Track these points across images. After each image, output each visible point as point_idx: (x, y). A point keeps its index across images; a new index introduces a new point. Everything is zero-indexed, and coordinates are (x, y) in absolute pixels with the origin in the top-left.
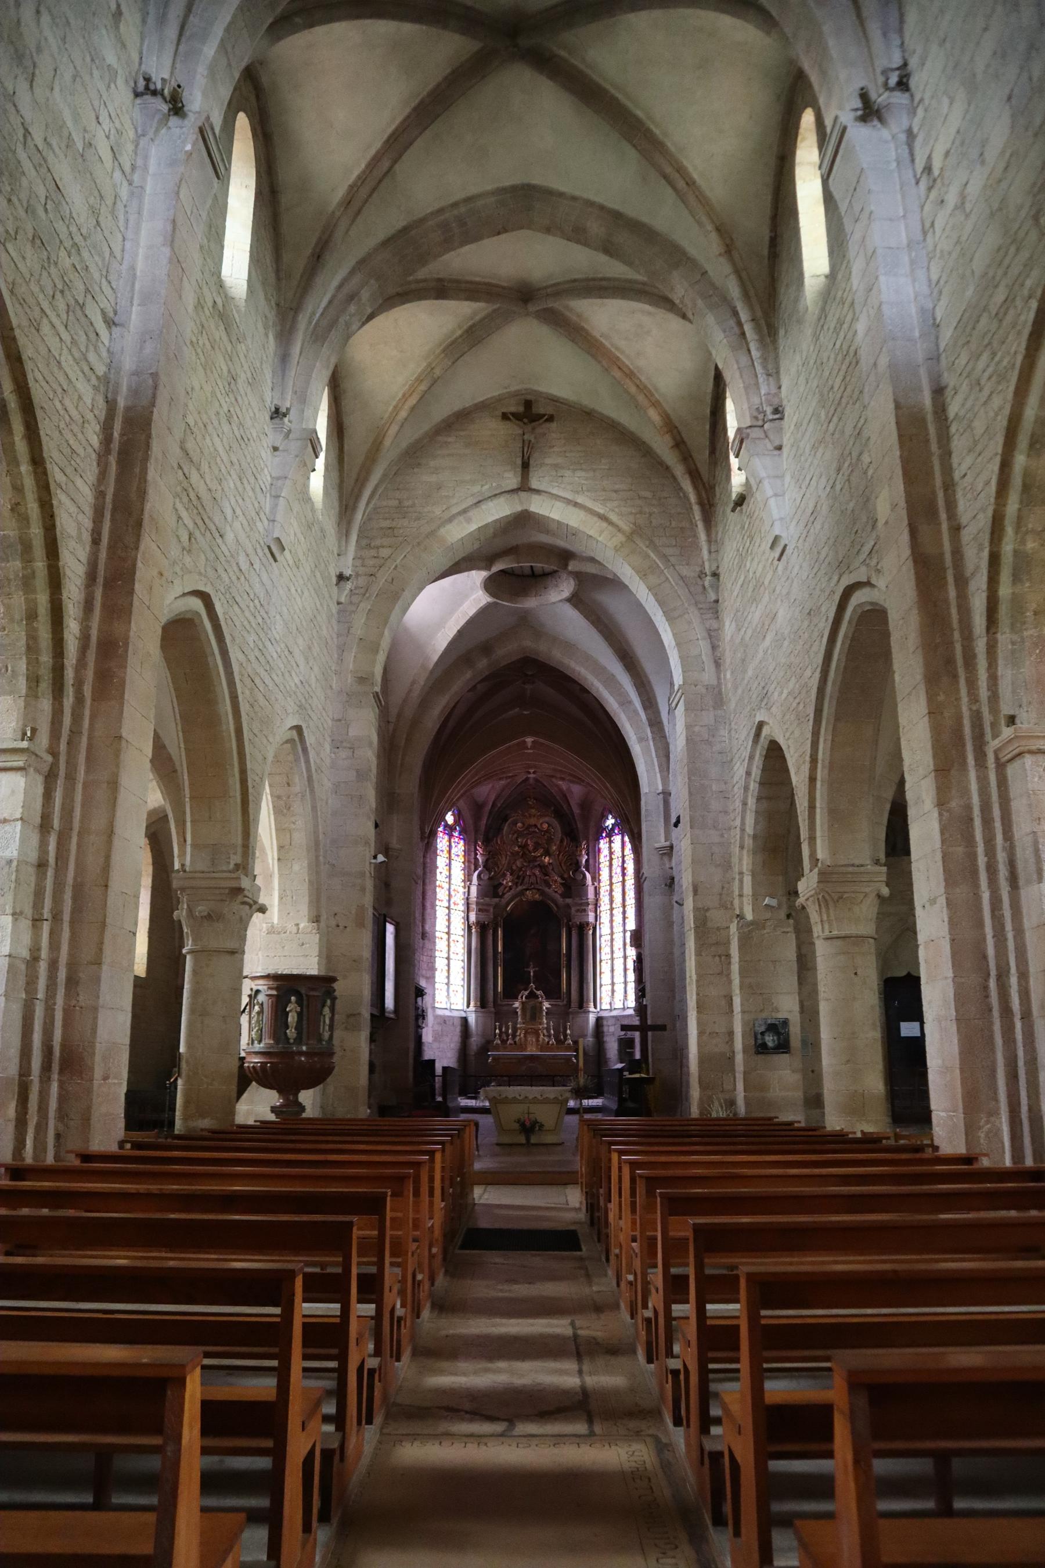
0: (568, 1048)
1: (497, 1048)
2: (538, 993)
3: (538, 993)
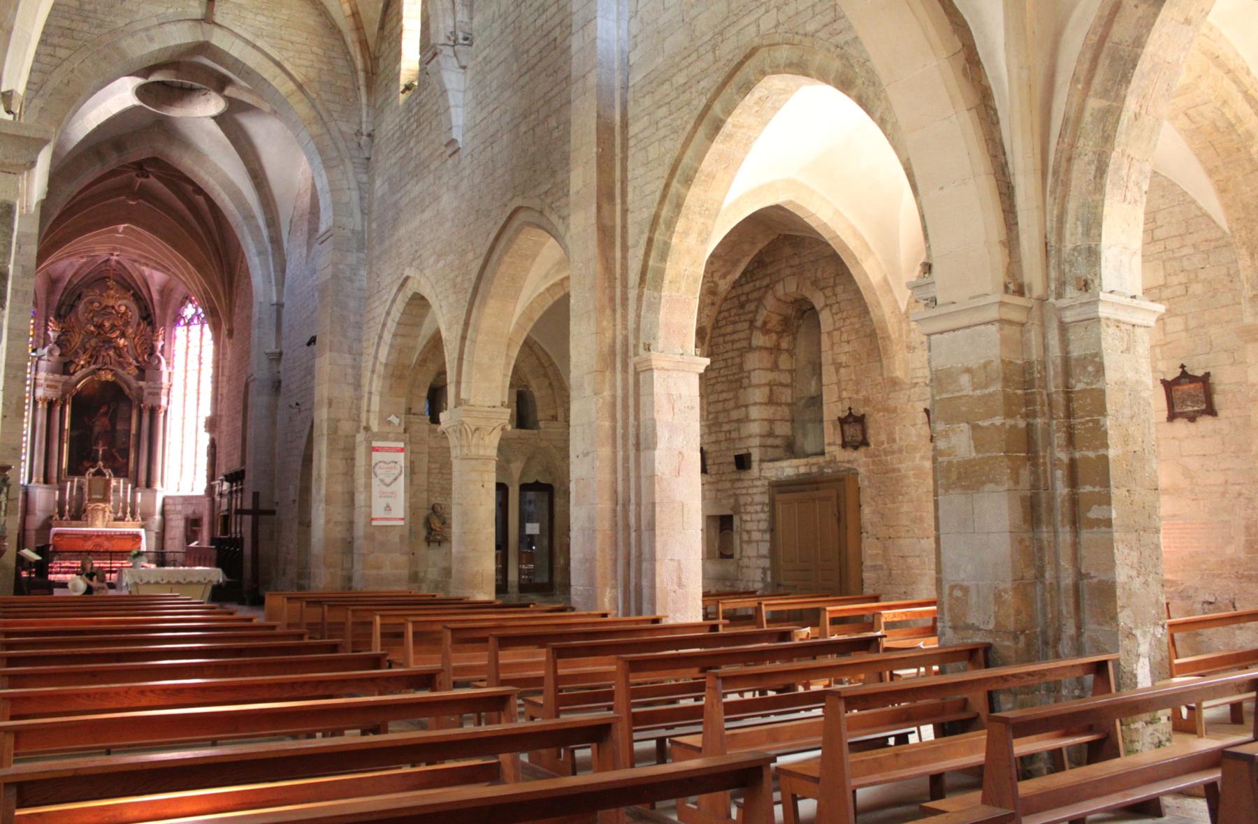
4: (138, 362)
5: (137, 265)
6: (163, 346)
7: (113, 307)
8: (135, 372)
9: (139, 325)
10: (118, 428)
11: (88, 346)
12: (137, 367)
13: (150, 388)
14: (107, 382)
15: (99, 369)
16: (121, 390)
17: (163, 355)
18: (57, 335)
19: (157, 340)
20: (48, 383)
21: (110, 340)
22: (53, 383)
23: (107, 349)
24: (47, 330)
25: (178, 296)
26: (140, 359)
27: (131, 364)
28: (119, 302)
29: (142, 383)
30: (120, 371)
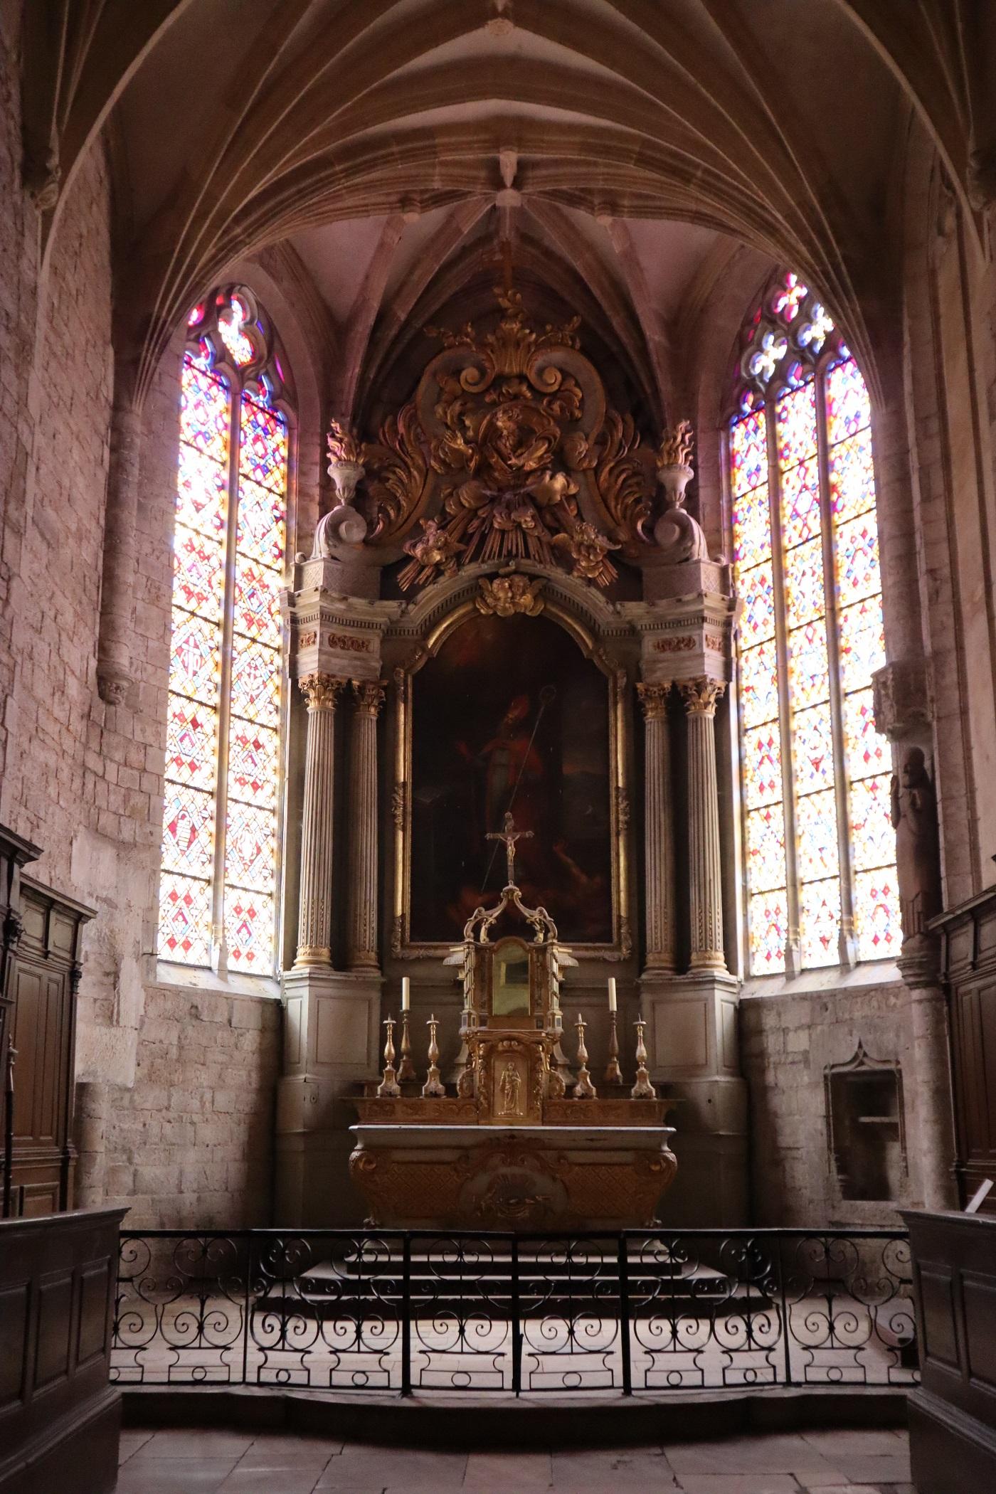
0: (642, 1110)
1: (385, 1109)
2: (535, 915)
3: (535, 915)
4: (612, 539)
5: (580, 215)
6: (692, 486)
7: (522, 378)
8: (607, 576)
9: (610, 423)
10: (569, 769)
11: (451, 509)
12: (610, 556)
13: (661, 623)
14: (521, 618)
15: (492, 577)
16: (567, 643)
17: (694, 511)
18: (355, 475)
19: (672, 465)
20: (339, 631)
21: (522, 475)
22: (349, 632)
23: (509, 508)
24: (326, 463)
25: (725, 323)
26: (623, 536)
27: (591, 548)
28: (539, 361)
29: (634, 610)
30: (558, 573)
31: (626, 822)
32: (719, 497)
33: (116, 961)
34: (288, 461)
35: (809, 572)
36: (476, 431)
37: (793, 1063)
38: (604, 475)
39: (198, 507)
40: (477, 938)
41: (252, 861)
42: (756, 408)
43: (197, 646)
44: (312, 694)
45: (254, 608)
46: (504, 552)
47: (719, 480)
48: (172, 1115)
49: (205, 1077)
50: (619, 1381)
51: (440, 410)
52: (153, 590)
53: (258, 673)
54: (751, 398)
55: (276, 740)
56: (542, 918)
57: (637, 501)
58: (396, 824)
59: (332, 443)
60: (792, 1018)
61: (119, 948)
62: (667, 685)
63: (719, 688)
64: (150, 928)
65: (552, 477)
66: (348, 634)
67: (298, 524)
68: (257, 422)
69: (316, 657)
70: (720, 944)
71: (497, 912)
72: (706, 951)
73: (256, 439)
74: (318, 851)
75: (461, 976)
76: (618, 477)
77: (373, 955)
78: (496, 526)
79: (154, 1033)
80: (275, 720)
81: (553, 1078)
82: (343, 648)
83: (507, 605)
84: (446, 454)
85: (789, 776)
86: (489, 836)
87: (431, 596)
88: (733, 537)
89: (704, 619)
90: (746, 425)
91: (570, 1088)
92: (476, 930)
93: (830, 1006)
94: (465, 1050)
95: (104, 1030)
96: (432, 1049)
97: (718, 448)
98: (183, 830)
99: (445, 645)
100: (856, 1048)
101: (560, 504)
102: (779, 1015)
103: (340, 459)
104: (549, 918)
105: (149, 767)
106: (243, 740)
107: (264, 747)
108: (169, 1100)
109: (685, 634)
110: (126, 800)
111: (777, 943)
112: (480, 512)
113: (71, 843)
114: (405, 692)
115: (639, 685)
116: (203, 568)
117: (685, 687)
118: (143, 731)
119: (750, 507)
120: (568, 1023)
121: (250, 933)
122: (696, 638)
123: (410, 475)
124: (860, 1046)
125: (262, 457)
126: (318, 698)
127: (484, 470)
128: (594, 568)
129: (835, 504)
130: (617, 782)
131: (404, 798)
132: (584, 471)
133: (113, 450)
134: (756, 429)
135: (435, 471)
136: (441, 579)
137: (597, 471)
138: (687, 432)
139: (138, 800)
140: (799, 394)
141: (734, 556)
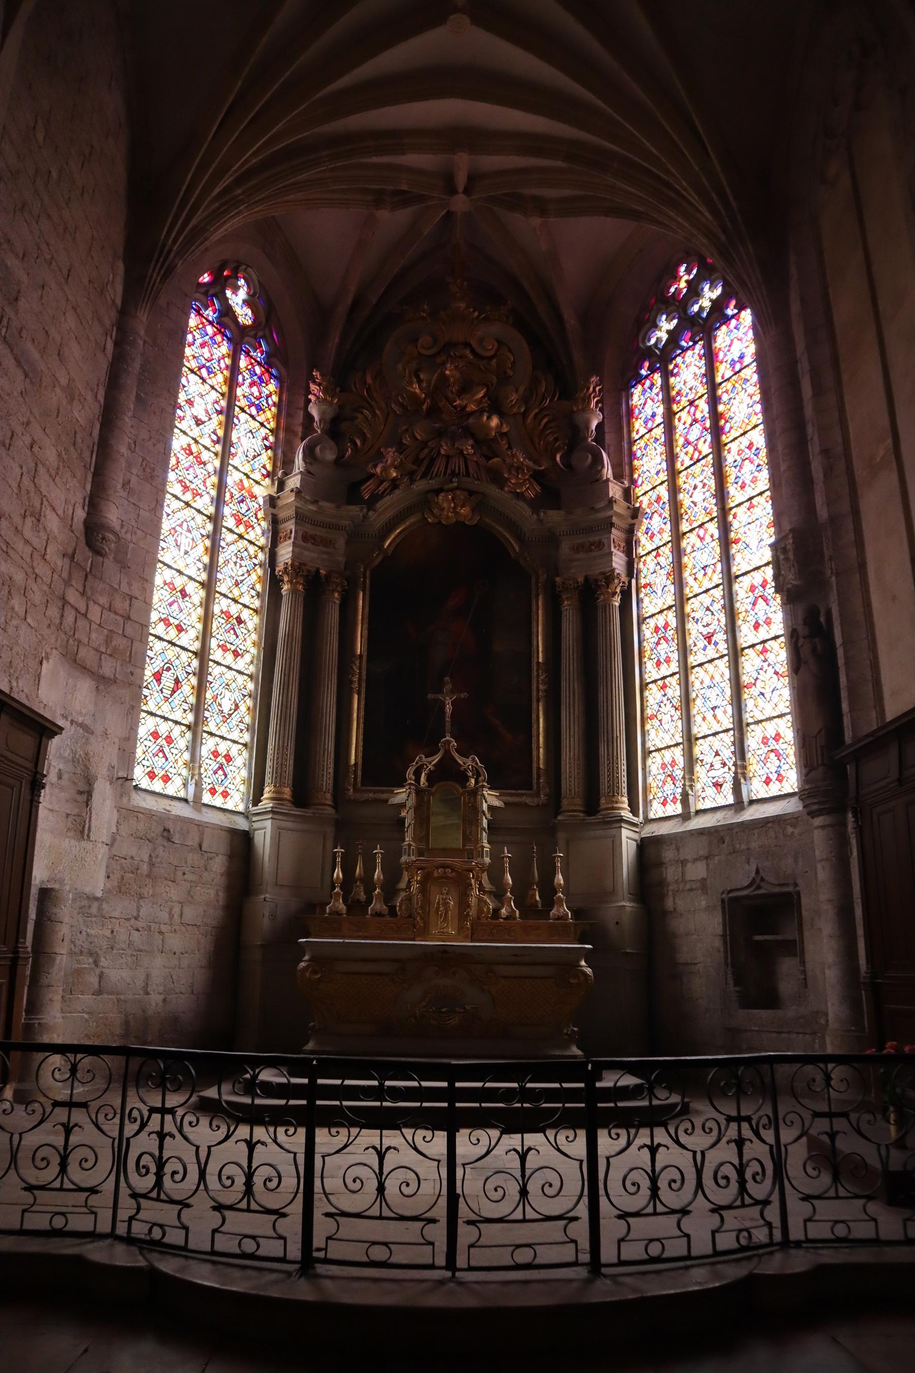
0: (560, 930)
1: (333, 925)
2: (468, 763)
3: (468, 763)
6: (600, 426)
7: (467, 345)
11: (407, 440)
15: (438, 492)
19: (586, 408)
22: (320, 532)
30: (493, 490)
31: (545, 691)
32: (621, 439)
33: (89, 781)
34: (278, 405)
35: (700, 485)
36: (429, 383)
37: (691, 890)
38: (529, 420)
39: (199, 422)
40: (418, 780)
41: (230, 715)
42: (652, 370)
43: (189, 531)
44: (286, 579)
45: (243, 511)
46: (449, 471)
47: (621, 428)
48: (140, 924)
49: (175, 893)
50: (585, 1258)
51: (400, 366)
52: (148, 470)
53: (243, 563)
54: (647, 364)
55: (256, 619)
56: (474, 764)
57: (556, 439)
58: (352, 688)
59: (313, 387)
60: (688, 852)
61: (93, 770)
62: (581, 580)
63: (623, 582)
64: (127, 757)
65: (489, 418)
66: (318, 533)
67: (283, 452)
68: (254, 371)
69: (291, 549)
70: (625, 791)
71: (436, 759)
72: (614, 796)
73: (252, 384)
74: (284, 707)
75: (403, 814)
76: (543, 418)
77: (329, 796)
78: (443, 453)
79: (127, 848)
80: (257, 603)
81: (480, 900)
82: (313, 544)
83: (450, 514)
84: (403, 398)
85: (684, 650)
86: (430, 696)
87: (388, 506)
88: (632, 469)
89: (612, 525)
90: (643, 385)
91: (496, 911)
92: (417, 774)
93: (727, 839)
94: (406, 876)
95: (73, 842)
96: (378, 874)
97: (620, 404)
98: (168, 680)
99: (398, 546)
100: (753, 874)
101: (495, 438)
102: (678, 849)
103: (318, 398)
104: (480, 764)
105: (133, 616)
106: (227, 615)
107: (245, 624)
108: (138, 911)
109: (596, 539)
110: (108, 640)
111: (673, 789)
112: (429, 444)
113: (41, 663)
114: (364, 582)
115: (558, 579)
116: (199, 470)
117: (596, 581)
118: (129, 584)
119: (647, 445)
120: (496, 856)
121: (226, 776)
122: (605, 541)
123: (374, 414)
124: (757, 872)
125: (258, 398)
126: (290, 582)
127: (434, 411)
128: (521, 485)
129: (723, 428)
130: (538, 658)
131: (360, 668)
132: (514, 414)
133: (117, 344)
134: (652, 385)
135: (395, 412)
136: (397, 492)
137: (525, 415)
138: (597, 386)
139: (119, 642)
140: (689, 353)
141: (633, 482)
